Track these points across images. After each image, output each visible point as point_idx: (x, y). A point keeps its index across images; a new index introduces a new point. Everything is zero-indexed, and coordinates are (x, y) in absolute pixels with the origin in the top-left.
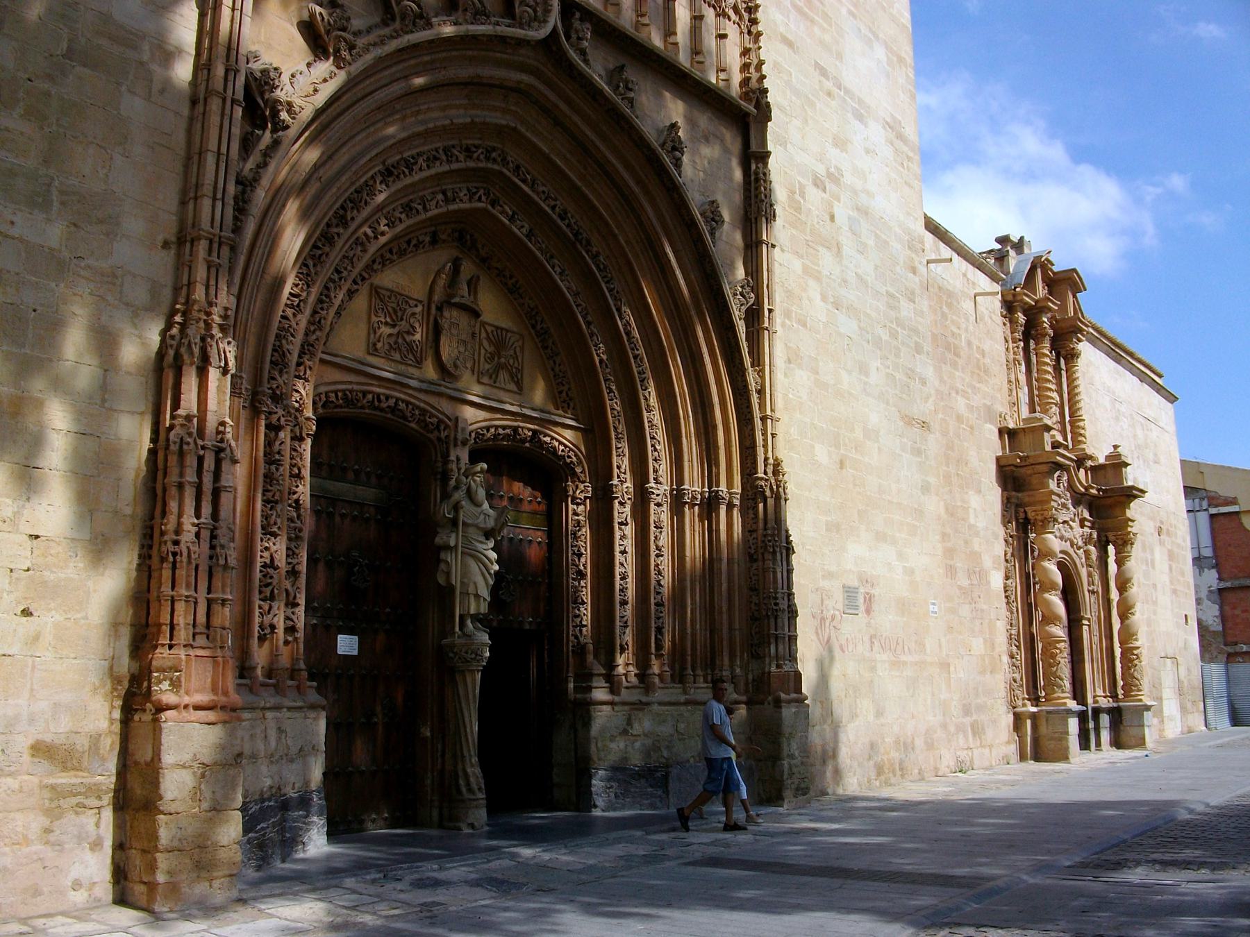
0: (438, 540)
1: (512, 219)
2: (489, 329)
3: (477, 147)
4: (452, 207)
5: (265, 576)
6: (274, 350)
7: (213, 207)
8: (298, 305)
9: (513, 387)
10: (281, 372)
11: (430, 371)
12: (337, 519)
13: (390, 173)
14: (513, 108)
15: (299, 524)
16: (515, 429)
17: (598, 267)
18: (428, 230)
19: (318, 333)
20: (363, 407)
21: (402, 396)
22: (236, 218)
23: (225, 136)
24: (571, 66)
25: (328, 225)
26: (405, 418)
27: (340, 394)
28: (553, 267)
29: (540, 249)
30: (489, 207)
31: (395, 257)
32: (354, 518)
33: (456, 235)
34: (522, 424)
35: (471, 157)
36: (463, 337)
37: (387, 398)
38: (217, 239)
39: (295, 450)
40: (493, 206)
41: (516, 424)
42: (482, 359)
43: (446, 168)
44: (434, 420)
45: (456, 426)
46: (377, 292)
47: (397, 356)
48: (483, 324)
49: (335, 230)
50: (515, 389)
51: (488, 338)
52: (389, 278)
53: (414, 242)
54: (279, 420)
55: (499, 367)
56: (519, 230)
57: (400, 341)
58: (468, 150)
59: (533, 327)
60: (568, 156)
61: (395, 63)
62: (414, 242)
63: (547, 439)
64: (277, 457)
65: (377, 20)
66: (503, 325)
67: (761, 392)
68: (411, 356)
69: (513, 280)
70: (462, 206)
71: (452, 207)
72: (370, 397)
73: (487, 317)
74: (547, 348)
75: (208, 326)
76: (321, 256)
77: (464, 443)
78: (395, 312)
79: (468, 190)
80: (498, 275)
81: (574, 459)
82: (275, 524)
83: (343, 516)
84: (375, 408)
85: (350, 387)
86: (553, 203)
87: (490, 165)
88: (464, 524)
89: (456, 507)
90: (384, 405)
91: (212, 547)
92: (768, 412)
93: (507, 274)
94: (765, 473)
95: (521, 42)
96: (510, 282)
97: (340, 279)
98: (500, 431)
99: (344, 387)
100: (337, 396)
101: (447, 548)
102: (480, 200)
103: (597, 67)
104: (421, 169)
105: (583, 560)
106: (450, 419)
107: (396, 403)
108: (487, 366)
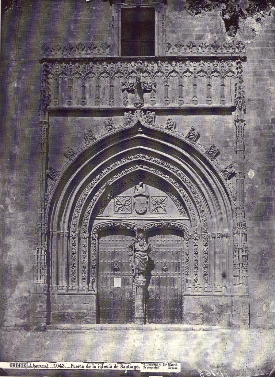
9: (164, 212)
63: (174, 224)
71: (127, 173)
81: (184, 228)
103: (161, 123)
107: (120, 224)
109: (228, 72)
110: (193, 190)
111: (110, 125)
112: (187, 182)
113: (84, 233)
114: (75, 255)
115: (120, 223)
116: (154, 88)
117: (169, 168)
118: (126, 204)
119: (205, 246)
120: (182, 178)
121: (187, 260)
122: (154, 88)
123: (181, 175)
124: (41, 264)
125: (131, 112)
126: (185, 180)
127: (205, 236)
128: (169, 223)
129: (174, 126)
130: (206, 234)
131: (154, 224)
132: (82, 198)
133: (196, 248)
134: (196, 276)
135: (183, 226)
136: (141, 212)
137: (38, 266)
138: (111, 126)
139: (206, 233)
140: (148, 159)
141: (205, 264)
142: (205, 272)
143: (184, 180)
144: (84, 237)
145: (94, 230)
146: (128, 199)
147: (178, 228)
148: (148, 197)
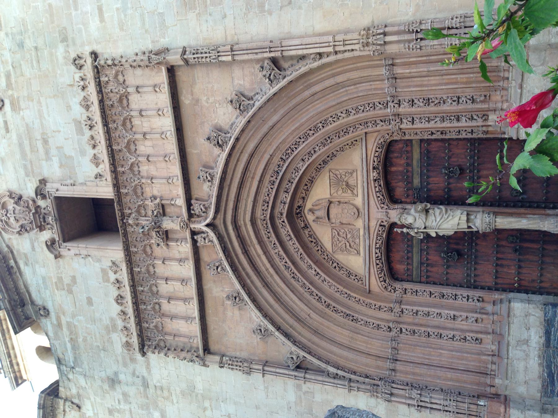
15: (435, 315)
16: (375, 180)
26: (382, 243)
32: (427, 254)
33: (299, 215)
34: (372, 178)
36: (340, 210)
41: (372, 182)
43: (280, 249)
50: (355, 174)
69: (307, 183)
70: (290, 230)
72: (378, 262)
75: (340, 109)
80: (308, 191)
83: (427, 259)
86: (270, 190)
88: (425, 228)
90: (380, 255)
92: (331, 49)
98: (377, 189)
103: (207, 190)
105: (435, 132)
109: (118, 81)
110: (312, 132)
112: (299, 142)
113: (392, 311)
114: (431, 333)
115: (376, 248)
116: (158, 200)
117: (278, 173)
118: (345, 236)
119: (413, 105)
120: (293, 151)
122: (158, 200)
124: (447, 406)
125: (195, 237)
126: (296, 146)
127: (394, 106)
128: (374, 168)
129: (207, 170)
130: (390, 104)
131: (376, 192)
133: (418, 121)
134: (475, 117)
135: (378, 144)
136: (357, 213)
137: (450, 412)
138: (217, 268)
139: (387, 104)
140: (268, 206)
141: (451, 103)
142: (468, 101)
143: (296, 148)
144: (400, 313)
145: (389, 290)
146: (337, 233)
148: (331, 203)
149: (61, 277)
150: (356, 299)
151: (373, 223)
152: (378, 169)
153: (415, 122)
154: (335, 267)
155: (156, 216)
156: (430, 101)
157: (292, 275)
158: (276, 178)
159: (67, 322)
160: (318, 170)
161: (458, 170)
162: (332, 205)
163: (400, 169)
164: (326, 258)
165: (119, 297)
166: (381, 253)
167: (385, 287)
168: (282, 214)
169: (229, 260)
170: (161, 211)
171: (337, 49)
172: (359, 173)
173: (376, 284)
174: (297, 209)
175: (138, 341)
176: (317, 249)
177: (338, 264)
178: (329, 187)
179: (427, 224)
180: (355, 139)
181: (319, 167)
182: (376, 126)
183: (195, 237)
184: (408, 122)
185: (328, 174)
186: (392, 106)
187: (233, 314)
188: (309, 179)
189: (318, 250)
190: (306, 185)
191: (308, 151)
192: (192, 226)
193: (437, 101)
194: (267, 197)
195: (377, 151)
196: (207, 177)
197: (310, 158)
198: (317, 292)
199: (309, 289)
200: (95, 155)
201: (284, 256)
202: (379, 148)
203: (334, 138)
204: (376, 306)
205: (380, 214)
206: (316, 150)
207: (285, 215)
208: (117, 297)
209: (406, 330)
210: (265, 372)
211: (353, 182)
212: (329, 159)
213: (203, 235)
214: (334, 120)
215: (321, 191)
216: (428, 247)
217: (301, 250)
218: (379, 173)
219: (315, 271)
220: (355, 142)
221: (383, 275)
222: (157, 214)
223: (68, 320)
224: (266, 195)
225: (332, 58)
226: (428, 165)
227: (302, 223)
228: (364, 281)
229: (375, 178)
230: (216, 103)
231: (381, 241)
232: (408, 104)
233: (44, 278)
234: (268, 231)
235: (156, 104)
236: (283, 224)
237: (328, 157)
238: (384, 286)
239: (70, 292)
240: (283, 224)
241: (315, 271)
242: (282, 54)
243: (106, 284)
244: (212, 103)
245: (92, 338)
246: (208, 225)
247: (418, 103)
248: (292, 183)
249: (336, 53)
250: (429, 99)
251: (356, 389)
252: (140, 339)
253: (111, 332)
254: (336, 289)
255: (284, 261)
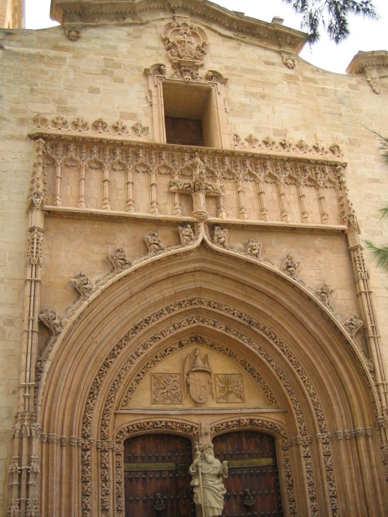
0: (192, 484)
1: (214, 325)
2: (220, 376)
3: (184, 301)
4: (179, 330)
5: (84, 514)
6: (84, 418)
7: (26, 374)
8: (93, 397)
9: (239, 400)
10: (87, 426)
11: (187, 404)
12: (148, 480)
13: (137, 328)
14: (198, 279)
15: (106, 488)
16: (239, 421)
17: (266, 333)
18: (176, 342)
19: (111, 404)
20: (149, 429)
21: (169, 420)
22: (36, 375)
23: (30, 345)
24: (218, 253)
25: (106, 359)
26: (172, 428)
27: (135, 426)
28: (243, 340)
29: (233, 334)
30: (201, 324)
31: (159, 359)
32: (157, 478)
33: (193, 339)
34: (242, 418)
35: (181, 307)
36: (203, 384)
37: (161, 422)
38: (27, 386)
39: (102, 456)
40: (203, 322)
41: (238, 418)
42: (218, 391)
43: (168, 316)
44: (189, 427)
45: (201, 428)
46: (154, 376)
47: (169, 402)
48: (216, 375)
49: (109, 361)
51: (220, 381)
52: (162, 367)
53: (169, 349)
54: (86, 446)
55: (229, 392)
56: (220, 329)
57: (169, 394)
58: (180, 304)
59: (246, 369)
60: (234, 289)
61: (121, 286)
62: (168, 350)
63: (260, 422)
64: (87, 462)
65: (109, 271)
66: (230, 373)
67: (373, 372)
68: (176, 400)
69: (229, 351)
71: (179, 330)
73: (215, 371)
74: (255, 377)
76: (102, 373)
77: (206, 434)
78: (165, 382)
79: (187, 320)
82: (87, 491)
83: (150, 478)
84: (157, 428)
85: (139, 422)
86: (232, 312)
87: (193, 307)
89: (197, 466)
90: (159, 426)
91: (26, 509)
92: (380, 381)
93: (225, 349)
94: (383, 415)
95: (190, 251)
96: (227, 352)
97: (120, 379)
98: (230, 424)
99: (136, 422)
100: (133, 427)
101: (194, 487)
102: (194, 322)
103: (235, 247)
104: (153, 321)
105: (291, 479)
106: (198, 425)
107: (166, 423)
108: (221, 394)
111: (156, 244)
120: (273, 339)
121: (290, 485)
123: (272, 334)
126: (278, 342)
127: (323, 439)
128: (251, 420)
131: (227, 423)
132: (102, 372)
139: (325, 432)
143: (276, 342)
144: (103, 448)
147: (267, 427)
149: (120, 68)
150: (113, 399)
151: (195, 420)
152: (249, 425)
153: (307, 459)
154: (139, 375)
155: (207, 189)
156: (331, 472)
157: (139, 327)
158: (244, 320)
159: (65, 58)
160: (243, 363)
161: (252, 504)
162: (208, 376)
163: (245, 447)
164: (149, 366)
165: (105, 125)
166: (160, 428)
167: (121, 432)
168: (203, 322)
169: (165, 259)
170: (212, 194)
171: (381, 387)
172: (241, 405)
173: (125, 422)
174: (201, 337)
175: (52, 134)
176: (158, 356)
177: (141, 379)
178: (224, 373)
179: (207, 476)
180: (278, 402)
181: (247, 364)
182: (299, 422)
183: (189, 226)
184: (306, 452)
185: (237, 373)
186: (324, 437)
187: (97, 253)
188: (233, 353)
189: (156, 357)
190: (227, 350)
191: (270, 354)
192: (202, 225)
193: (331, 477)
194: (224, 308)
195: (268, 423)
196: (255, 249)
197: (263, 355)
198: (121, 354)
199: (125, 344)
200: (258, 140)
201: (161, 320)
202: (271, 425)
203: (285, 381)
204: (107, 422)
205: (207, 424)
206: (272, 362)
207: (201, 324)
208: (105, 123)
209: (89, 456)
210: (33, 283)
211: (232, 398)
212: (256, 374)
213: (192, 235)
214: (306, 382)
215: (219, 365)
216: (164, 478)
217: (163, 339)
218: (246, 425)
219: (142, 353)
220: (274, 401)
221: (136, 429)
222: (209, 190)
223: (68, 60)
224: (226, 307)
225: (373, 383)
226: (251, 475)
227: (186, 342)
228: (125, 408)
229: (242, 421)
230: (319, 269)
231: (174, 427)
232: (327, 451)
233: (115, 48)
234: (187, 305)
235: (311, 213)
236: (192, 322)
237: (258, 374)
238: (123, 430)
239: (104, 72)
240: (192, 322)
241: (142, 353)
242: (372, 337)
243: (118, 115)
244: (319, 266)
245: (47, 80)
246: (203, 241)
247: (329, 461)
248: (236, 336)
249: (377, 386)
250: (331, 470)
251: (27, 394)
252: (55, 137)
253: (57, 105)
254: (122, 376)
255: (155, 319)
